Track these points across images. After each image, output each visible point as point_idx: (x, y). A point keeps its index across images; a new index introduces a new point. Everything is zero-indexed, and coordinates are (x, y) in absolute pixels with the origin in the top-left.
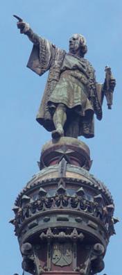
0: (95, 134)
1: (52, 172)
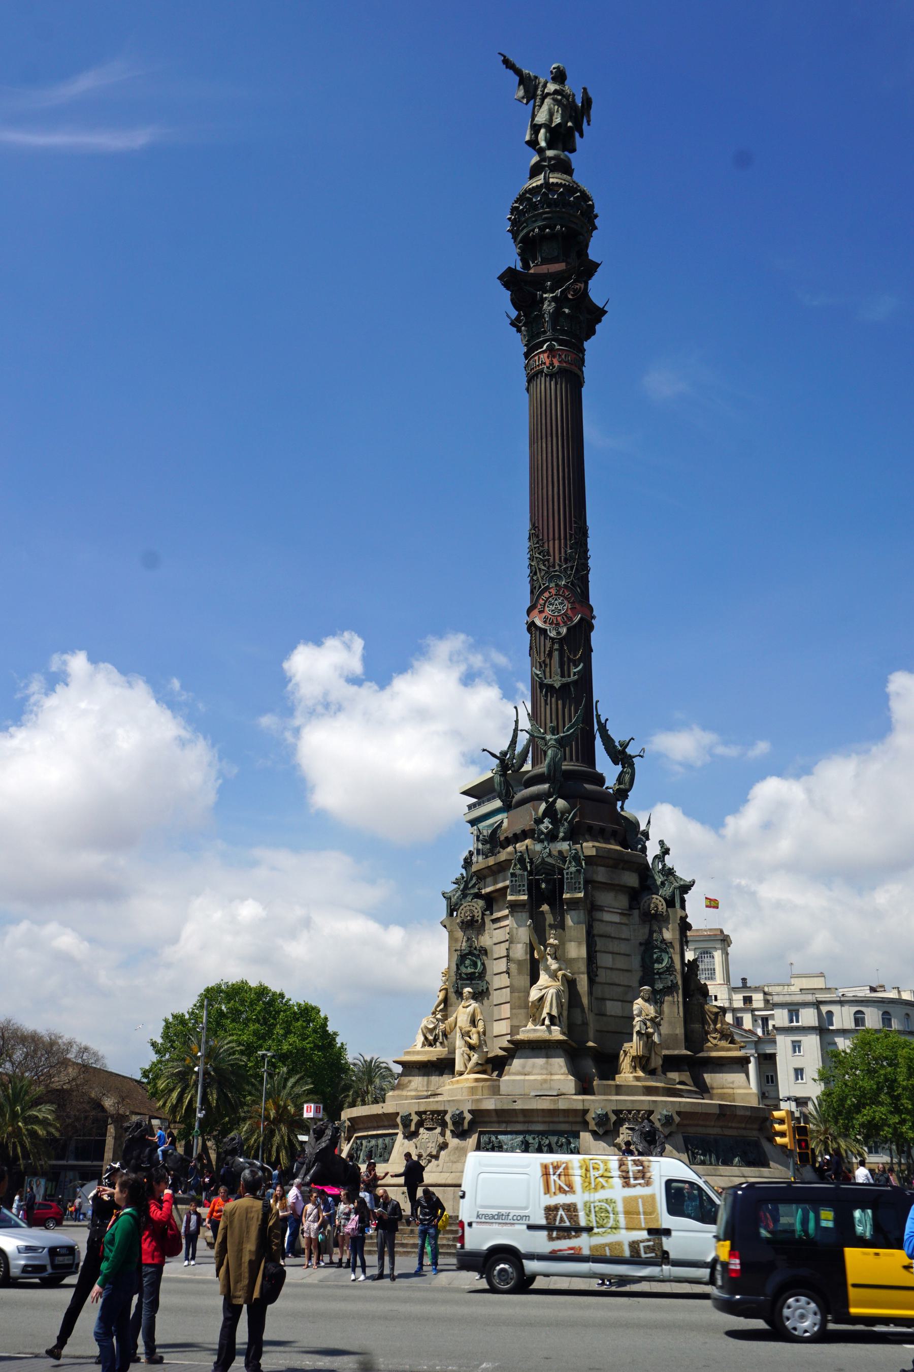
0: (578, 149)
1: (539, 180)
